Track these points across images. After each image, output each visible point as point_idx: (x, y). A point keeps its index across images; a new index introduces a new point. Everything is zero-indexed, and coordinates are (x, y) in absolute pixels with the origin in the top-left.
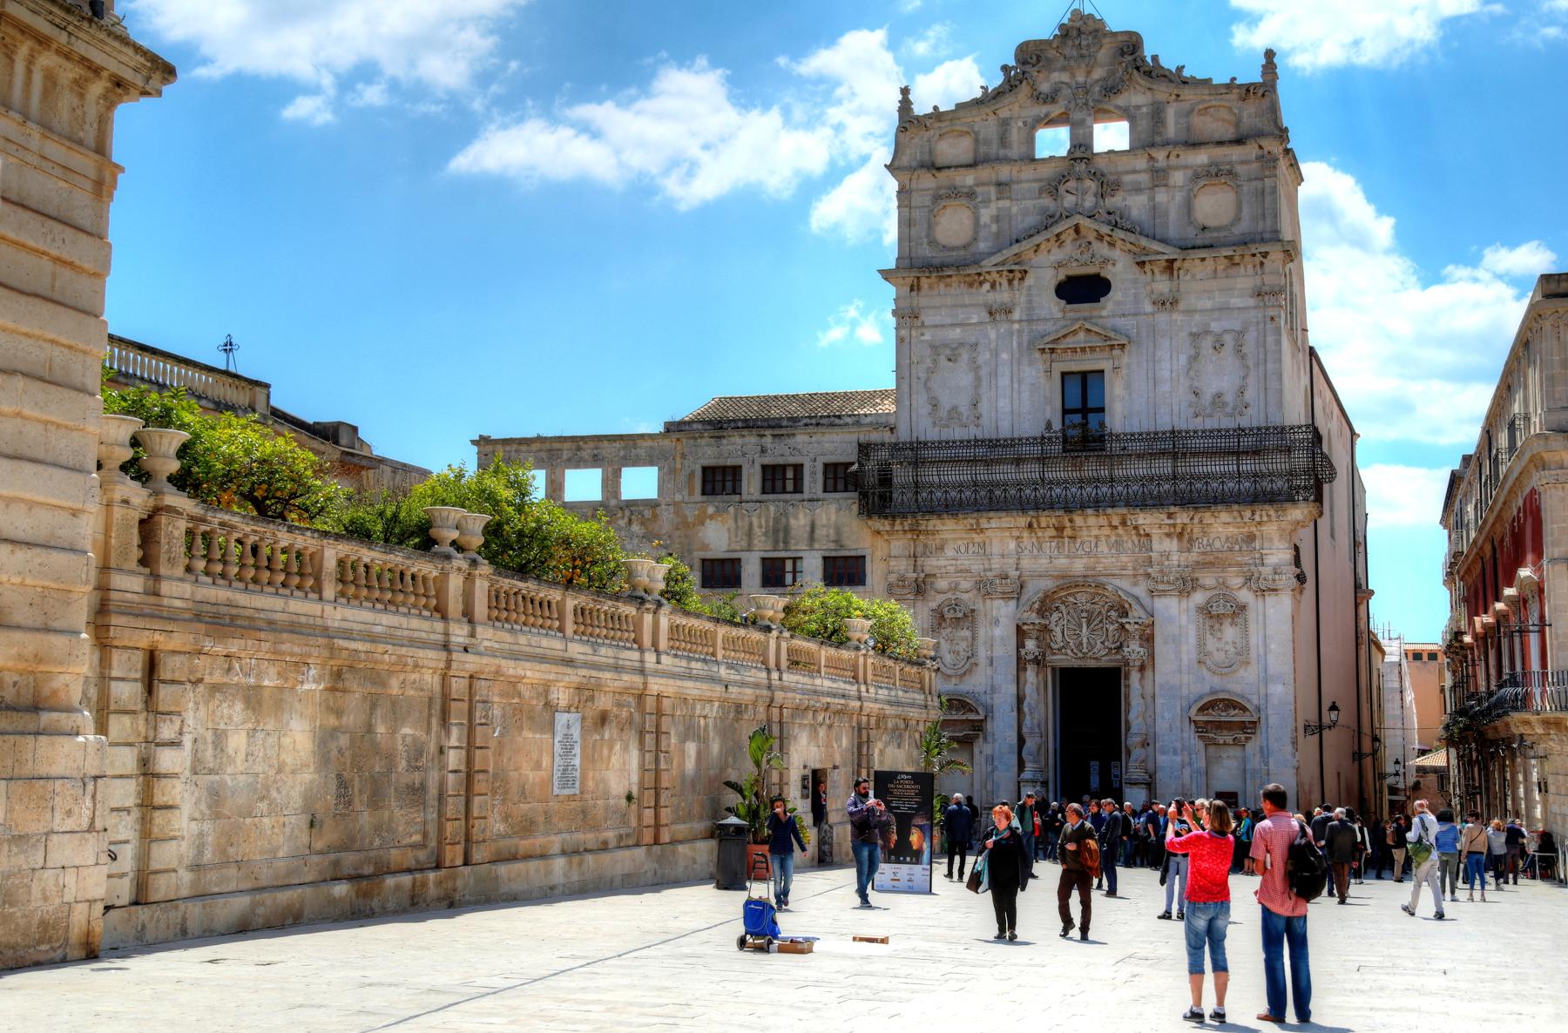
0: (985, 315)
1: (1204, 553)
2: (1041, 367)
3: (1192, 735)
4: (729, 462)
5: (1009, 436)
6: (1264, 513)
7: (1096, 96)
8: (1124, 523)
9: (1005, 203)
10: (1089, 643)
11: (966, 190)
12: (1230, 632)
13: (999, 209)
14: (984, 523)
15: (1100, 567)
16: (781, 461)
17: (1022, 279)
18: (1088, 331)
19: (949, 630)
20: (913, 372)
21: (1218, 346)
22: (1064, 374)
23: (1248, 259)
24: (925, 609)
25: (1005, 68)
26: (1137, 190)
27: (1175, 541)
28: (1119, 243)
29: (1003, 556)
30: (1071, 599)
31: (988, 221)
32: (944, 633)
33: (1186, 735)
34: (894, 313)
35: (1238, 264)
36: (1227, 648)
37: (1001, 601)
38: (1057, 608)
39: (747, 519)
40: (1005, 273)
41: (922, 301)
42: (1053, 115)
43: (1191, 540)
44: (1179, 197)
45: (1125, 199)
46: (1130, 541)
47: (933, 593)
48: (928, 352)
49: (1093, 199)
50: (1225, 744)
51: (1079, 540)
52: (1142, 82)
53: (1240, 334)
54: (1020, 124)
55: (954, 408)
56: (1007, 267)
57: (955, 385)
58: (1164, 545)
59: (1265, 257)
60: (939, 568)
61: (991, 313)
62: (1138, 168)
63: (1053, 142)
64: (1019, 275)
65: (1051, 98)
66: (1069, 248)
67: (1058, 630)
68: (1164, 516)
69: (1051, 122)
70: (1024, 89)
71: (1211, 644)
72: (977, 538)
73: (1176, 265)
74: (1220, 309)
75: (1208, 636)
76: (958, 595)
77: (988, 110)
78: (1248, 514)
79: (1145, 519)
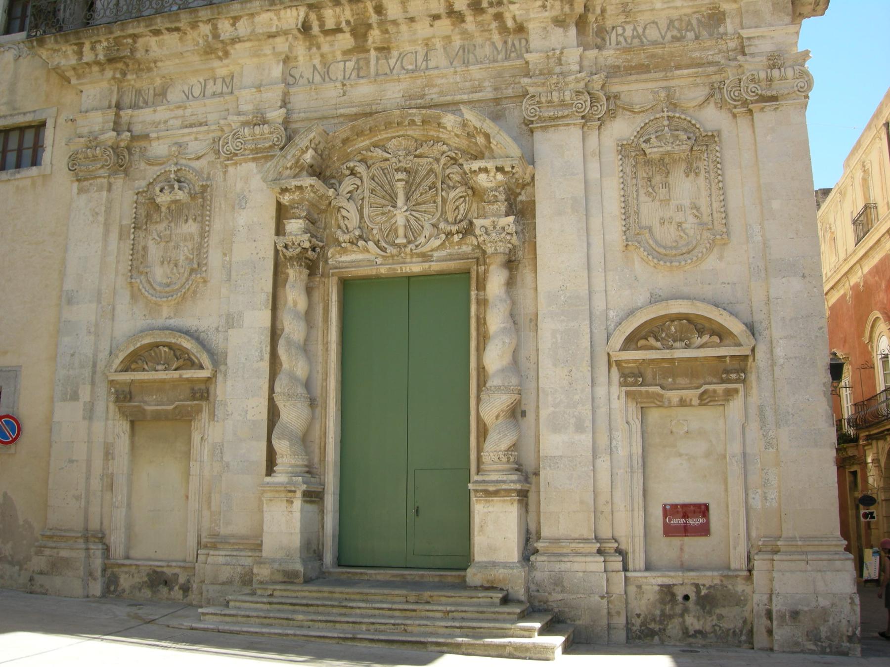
1: (628, 50)
3: (615, 390)
10: (408, 226)
14: (225, 28)
15: (433, 95)
19: (164, 224)
27: (573, 31)
29: (259, 88)
30: (378, 153)
33: (601, 391)
36: (680, 216)
37: (252, 165)
38: (353, 173)
43: (601, 32)
47: (143, 165)
50: (683, 403)
51: (395, 53)
60: (156, 124)
72: (222, 69)
75: (643, 198)
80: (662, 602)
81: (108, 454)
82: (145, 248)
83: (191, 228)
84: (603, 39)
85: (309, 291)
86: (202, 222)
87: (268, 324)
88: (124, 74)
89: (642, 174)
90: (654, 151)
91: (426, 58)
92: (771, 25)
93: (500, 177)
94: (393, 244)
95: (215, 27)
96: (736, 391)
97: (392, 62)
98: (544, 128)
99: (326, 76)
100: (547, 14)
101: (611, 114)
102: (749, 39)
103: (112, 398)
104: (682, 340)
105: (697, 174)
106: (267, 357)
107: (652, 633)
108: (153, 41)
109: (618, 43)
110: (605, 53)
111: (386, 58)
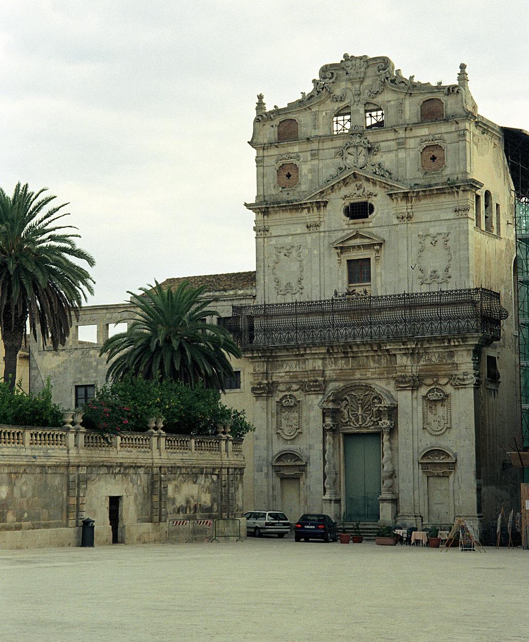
0: (305, 227)
3: (420, 471)
5: (318, 299)
9: (316, 162)
12: (441, 410)
17: (325, 206)
19: (287, 413)
21: (434, 243)
24: (273, 403)
25: (314, 81)
31: (306, 172)
33: (416, 471)
34: (255, 229)
37: (314, 396)
38: (346, 399)
45: (382, 157)
47: (277, 392)
48: (274, 251)
50: (439, 476)
54: (324, 114)
57: (289, 270)
61: (308, 227)
71: (431, 417)
82: (281, 421)
85: (333, 438)
86: (299, 413)
89: (429, 406)
93: (386, 409)
105: (444, 406)
106: (322, 458)
109: (423, 361)
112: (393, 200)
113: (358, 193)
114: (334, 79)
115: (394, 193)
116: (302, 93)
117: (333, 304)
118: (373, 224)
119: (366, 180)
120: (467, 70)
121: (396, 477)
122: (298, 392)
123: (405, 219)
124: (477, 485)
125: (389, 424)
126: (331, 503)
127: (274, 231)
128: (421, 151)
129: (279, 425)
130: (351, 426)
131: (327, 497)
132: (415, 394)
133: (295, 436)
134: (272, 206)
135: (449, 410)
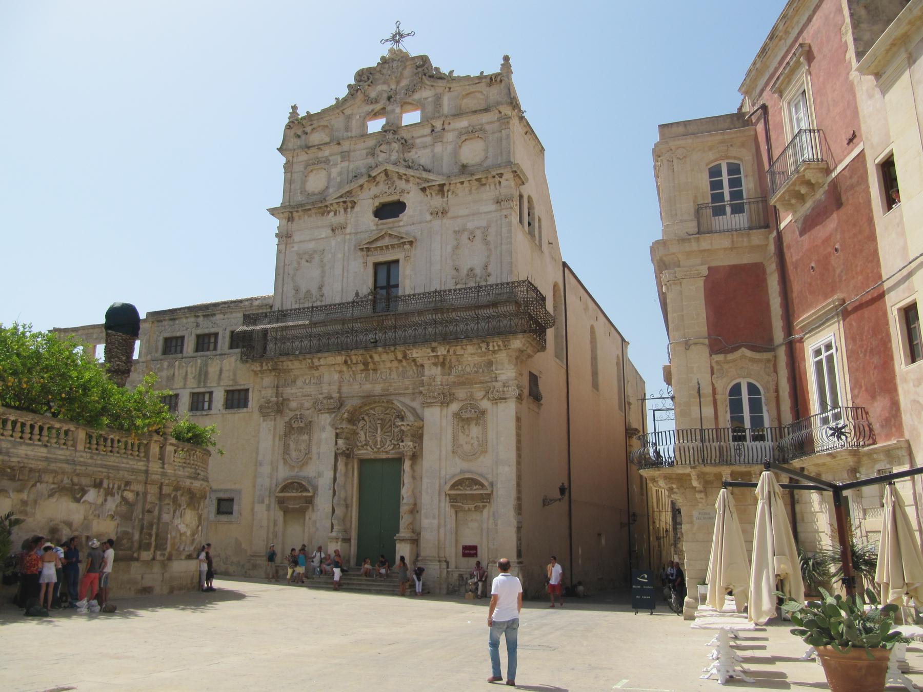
0: (329, 231)
1: (458, 376)
2: (361, 261)
3: (448, 504)
4: (178, 334)
6: (495, 344)
7: (402, 95)
8: (405, 357)
9: (346, 164)
10: (382, 441)
11: (324, 159)
12: (475, 430)
13: (342, 168)
14: (316, 362)
15: (391, 390)
16: (206, 331)
17: (353, 207)
18: (391, 235)
19: (296, 435)
20: (286, 270)
21: (472, 238)
22: (377, 265)
23: (490, 180)
24: (281, 423)
25: (349, 86)
26: (425, 147)
27: (439, 368)
28: (411, 179)
30: (372, 412)
32: (293, 437)
33: (443, 504)
34: (277, 235)
35: (485, 185)
36: (472, 441)
37: (327, 415)
38: (363, 419)
39: (185, 368)
40: (341, 204)
41: (294, 226)
42: (376, 110)
43: (451, 368)
44: (450, 148)
46: (412, 371)
47: (287, 411)
49: (396, 154)
50: (469, 510)
51: (379, 372)
52: (427, 82)
53: (487, 228)
54: (358, 117)
55: (308, 291)
56: (342, 200)
57: (309, 278)
58: (433, 372)
59: (501, 177)
60: (292, 394)
61: (333, 230)
62: (425, 134)
63: (375, 126)
64: (350, 205)
65: (376, 101)
66: (382, 187)
67: (362, 433)
68: (429, 350)
69: (375, 115)
70: (360, 95)
71: (462, 439)
72: (316, 373)
73: (446, 188)
74: (474, 214)
75: (460, 433)
76: (303, 412)
77: (338, 111)
78: (484, 346)
79: (416, 353)
80: (459, 580)
81: (275, 524)
82: (289, 444)
83: (305, 437)
84: (451, 371)
85: (346, 465)
87: (332, 476)
88: (279, 373)
90: (465, 415)
91: (390, 375)
92: (507, 369)
93: (408, 427)
94: (376, 447)
95: (312, 360)
96: (486, 506)
97: (378, 375)
98: (428, 406)
99: (355, 379)
100: (429, 362)
101: (451, 401)
102: (499, 374)
103: (277, 502)
104: (469, 487)
106: (332, 489)
107: (456, 591)
108: (289, 363)
109: (456, 372)
110: (450, 377)
111: (376, 374)
112: (427, 196)
113: (389, 191)
114: (370, 81)
115: (429, 187)
116: (336, 99)
117: (353, 307)
118: (404, 223)
119: (398, 178)
120: (510, 62)
121: (417, 512)
122: (310, 411)
123: (440, 214)
124: (518, 522)
125: (411, 446)
126: (337, 542)
127: (297, 237)
128: (460, 144)
129: (286, 450)
130: (367, 449)
131: (334, 534)
132: (444, 412)
133: (303, 462)
134: (296, 210)
135: (485, 432)
